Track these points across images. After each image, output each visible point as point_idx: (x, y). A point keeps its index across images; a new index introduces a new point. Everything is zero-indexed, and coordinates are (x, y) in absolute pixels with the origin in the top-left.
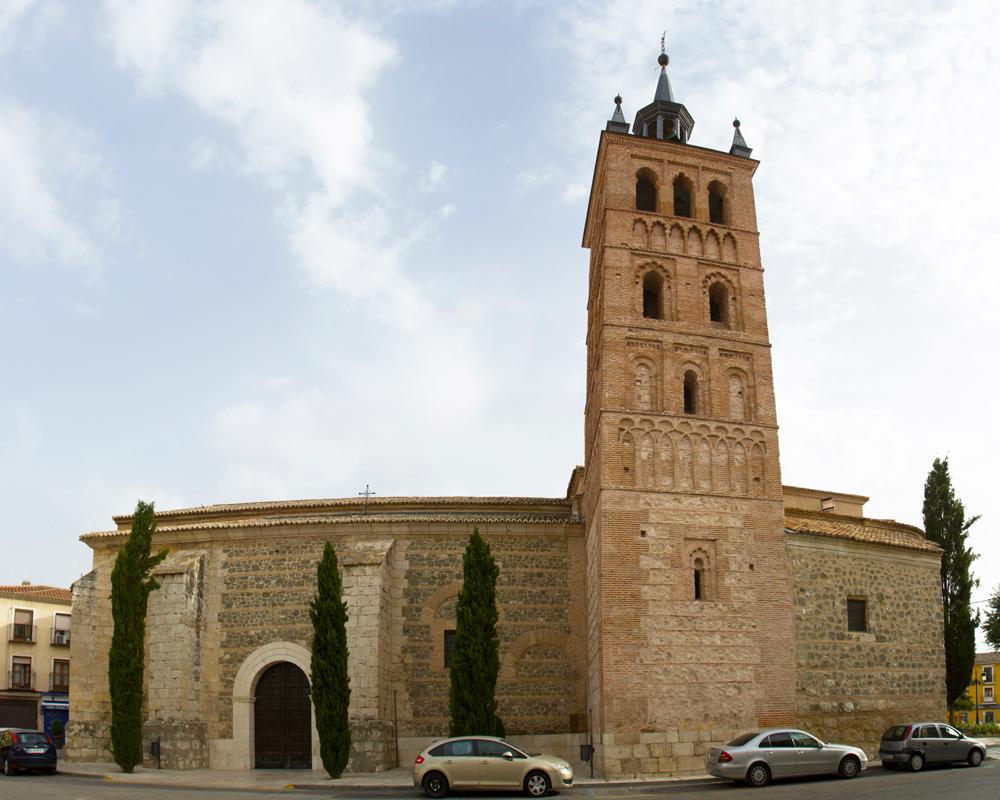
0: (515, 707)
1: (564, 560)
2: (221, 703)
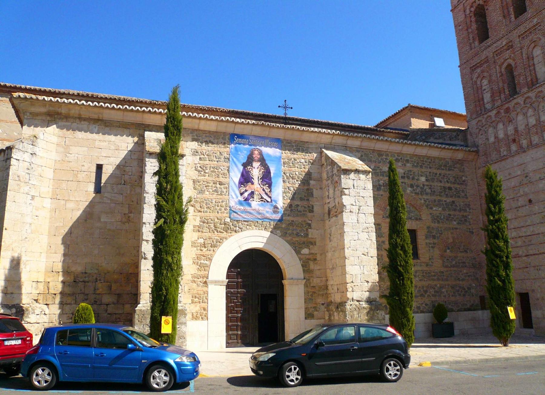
0: (444, 290)
1: (464, 178)
2: (194, 285)
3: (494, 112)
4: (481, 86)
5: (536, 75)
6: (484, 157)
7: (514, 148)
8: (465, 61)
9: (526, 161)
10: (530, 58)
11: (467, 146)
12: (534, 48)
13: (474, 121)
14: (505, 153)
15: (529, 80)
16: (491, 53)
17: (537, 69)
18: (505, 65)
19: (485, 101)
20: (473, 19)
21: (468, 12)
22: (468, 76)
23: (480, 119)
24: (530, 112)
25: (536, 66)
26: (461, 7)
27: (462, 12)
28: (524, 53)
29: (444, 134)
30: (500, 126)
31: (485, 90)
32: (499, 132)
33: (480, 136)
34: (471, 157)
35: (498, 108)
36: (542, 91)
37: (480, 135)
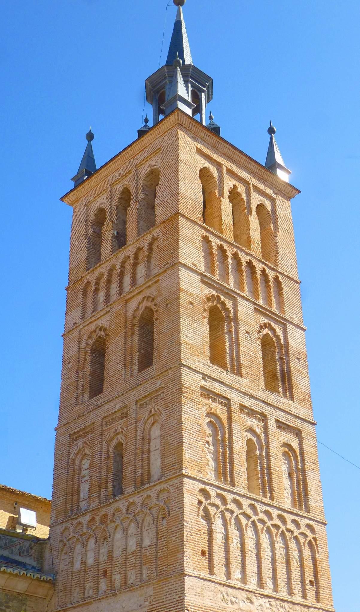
4: (80, 469)
5: (149, 468)
6: (61, 594)
7: (103, 585)
8: (65, 422)
10: (146, 440)
11: (40, 571)
12: (153, 424)
15: (139, 474)
16: (100, 419)
19: (82, 496)
20: (89, 358)
21: (83, 344)
23: (67, 525)
24: (132, 529)
25: (152, 454)
26: (76, 334)
27: (75, 343)
28: (138, 429)
29: (12, 542)
30: (92, 543)
31: (84, 476)
33: (63, 557)
34: (42, 590)
35: (93, 513)
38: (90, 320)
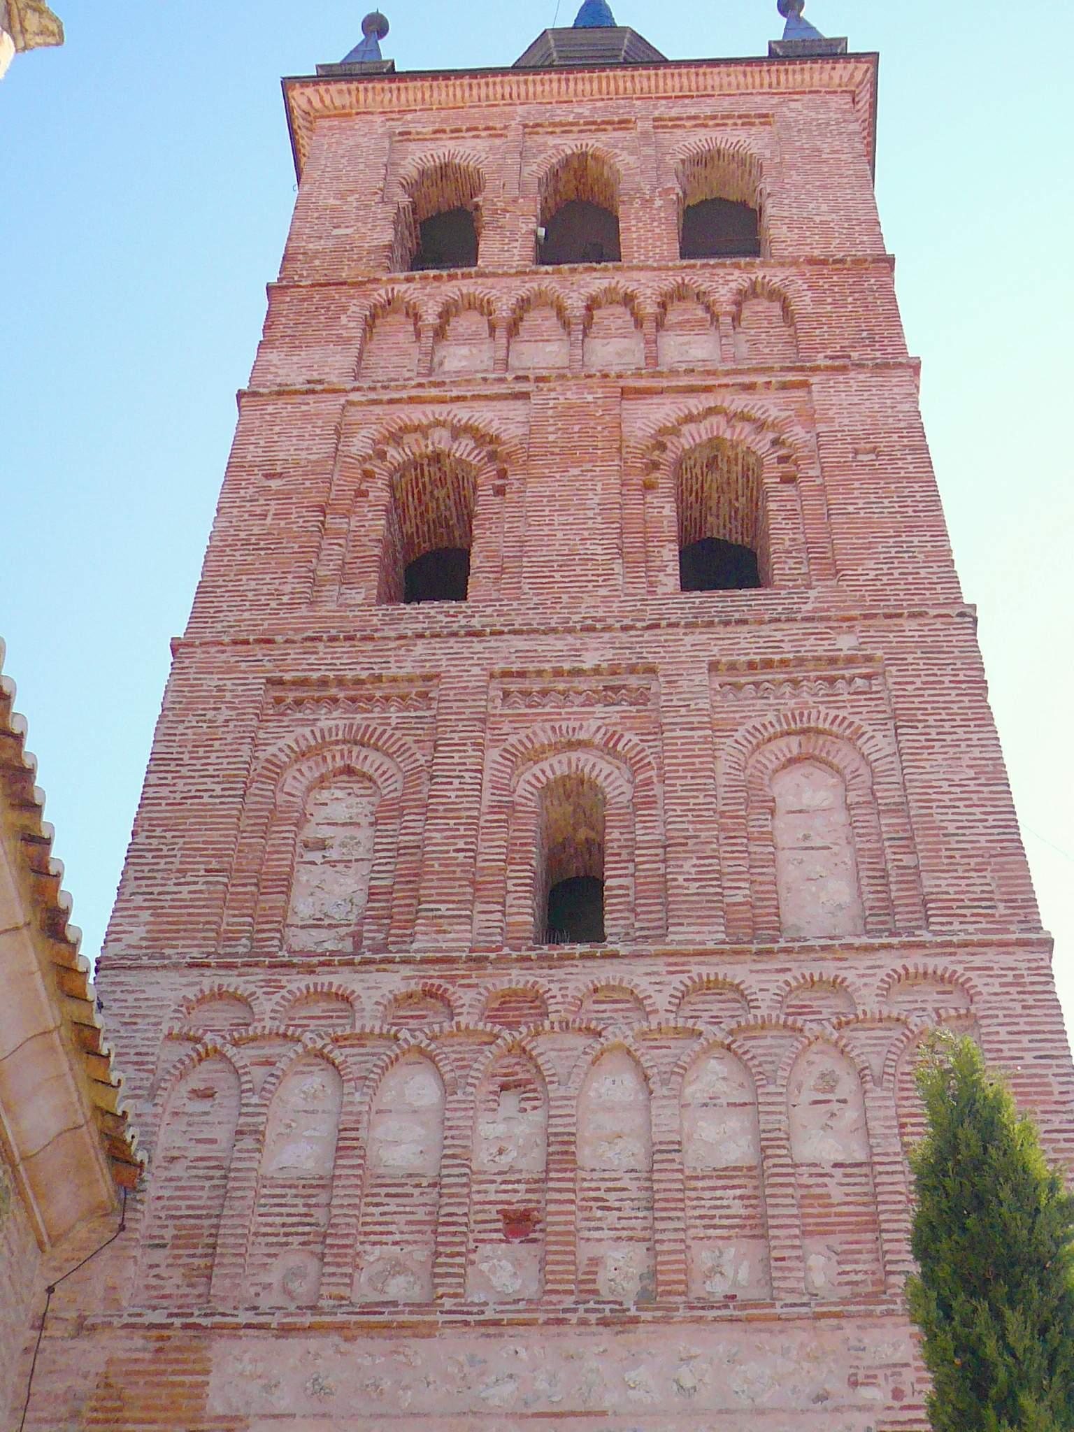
3: (395, 981)
6: (159, 1256)
9: (609, 1401)
13: (174, 977)
14: (397, 1288)
17: (790, 873)
18: (557, 766)
22: (225, 713)
32: (385, 1129)
35: (433, 970)
36: (837, 986)
37: (184, 1088)
38: (414, 393)
